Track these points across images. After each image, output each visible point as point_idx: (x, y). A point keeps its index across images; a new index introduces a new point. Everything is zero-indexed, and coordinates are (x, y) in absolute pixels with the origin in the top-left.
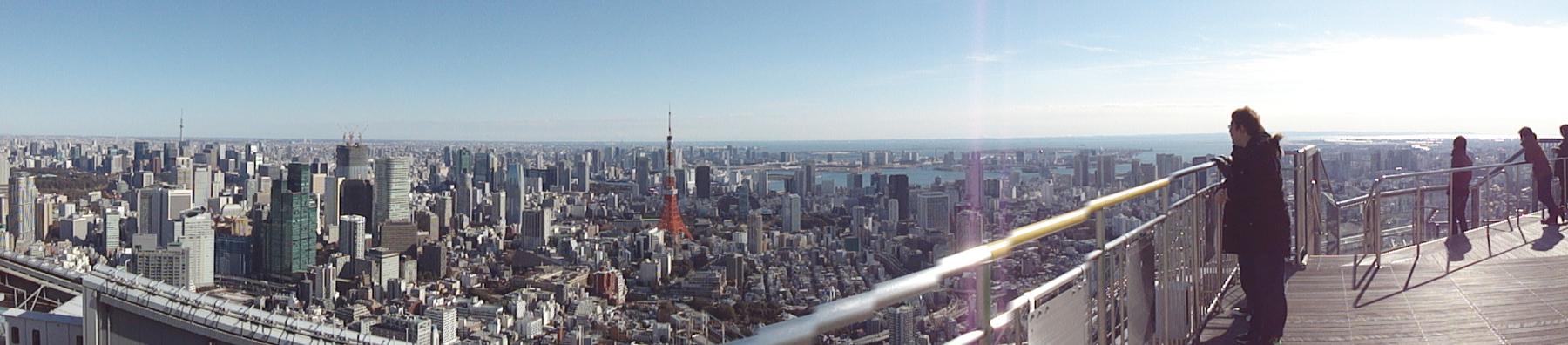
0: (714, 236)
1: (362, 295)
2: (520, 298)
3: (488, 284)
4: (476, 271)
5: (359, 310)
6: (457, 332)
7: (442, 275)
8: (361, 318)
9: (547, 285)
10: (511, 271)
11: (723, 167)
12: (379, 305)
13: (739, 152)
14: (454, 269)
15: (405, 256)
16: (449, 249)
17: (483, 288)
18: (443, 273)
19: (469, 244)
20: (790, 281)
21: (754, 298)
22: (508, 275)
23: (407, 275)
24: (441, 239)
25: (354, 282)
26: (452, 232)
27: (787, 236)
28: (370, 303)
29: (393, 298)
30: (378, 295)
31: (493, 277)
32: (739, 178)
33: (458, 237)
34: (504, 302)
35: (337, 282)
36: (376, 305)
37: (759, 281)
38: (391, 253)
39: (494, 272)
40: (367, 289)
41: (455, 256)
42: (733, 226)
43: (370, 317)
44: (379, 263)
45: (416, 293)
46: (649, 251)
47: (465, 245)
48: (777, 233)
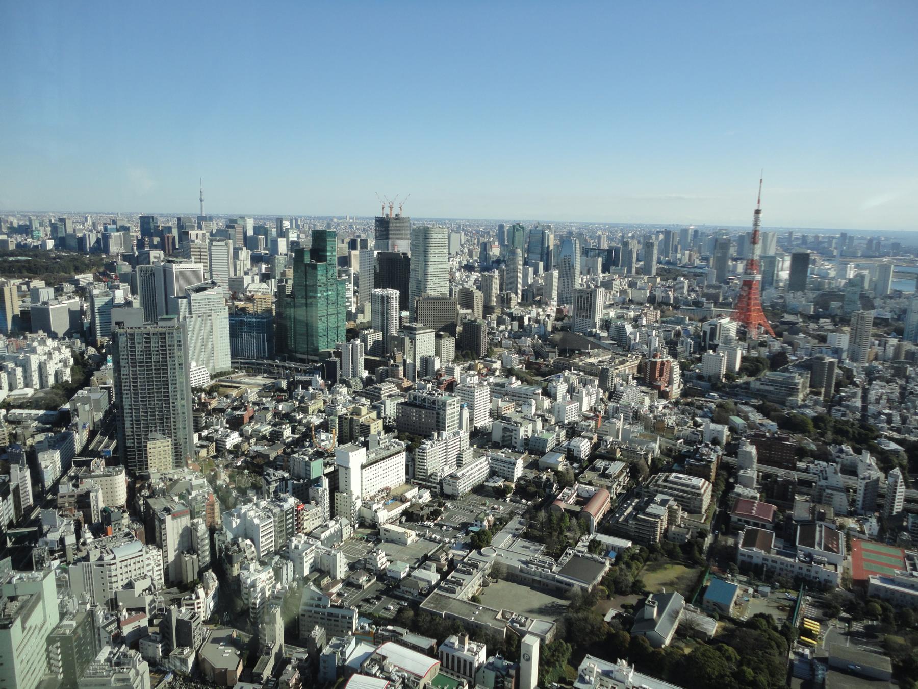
0: (801, 335)
1: (391, 373)
2: (561, 380)
3: (529, 365)
4: (520, 352)
6: (490, 413)
7: (482, 355)
8: (390, 396)
9: (591, 371)
11: (829, 256)
12: (411, 384)
13: (856, 242)
14: (496, 349)
15: (441, 333)
16: (493, 329)
18: (483, 352)
19: (516, 324)
20: (901, 403)
21: (844, 415)
23: (444, 352)
24: (484, 318)
25: (383, 360)
26: (498, 312)
27: (908, 346)
28: (400, 381)
29: (426, 376)
31: (537, 359)
32: (851, 272)
33: (504, 317)
34: (545, 384)
35: (365, 359)
36: (406, 383)
37: (854, 395)
38: (427, 328)
39: (538, 354)
40: (397, 366)
41: (498, 335)
42: (832, 327)
43: (398, 395)
44: (413, 340)
45: (450, 371)
46: (716, 342)
47: (511, 324)
48: (893, 341)
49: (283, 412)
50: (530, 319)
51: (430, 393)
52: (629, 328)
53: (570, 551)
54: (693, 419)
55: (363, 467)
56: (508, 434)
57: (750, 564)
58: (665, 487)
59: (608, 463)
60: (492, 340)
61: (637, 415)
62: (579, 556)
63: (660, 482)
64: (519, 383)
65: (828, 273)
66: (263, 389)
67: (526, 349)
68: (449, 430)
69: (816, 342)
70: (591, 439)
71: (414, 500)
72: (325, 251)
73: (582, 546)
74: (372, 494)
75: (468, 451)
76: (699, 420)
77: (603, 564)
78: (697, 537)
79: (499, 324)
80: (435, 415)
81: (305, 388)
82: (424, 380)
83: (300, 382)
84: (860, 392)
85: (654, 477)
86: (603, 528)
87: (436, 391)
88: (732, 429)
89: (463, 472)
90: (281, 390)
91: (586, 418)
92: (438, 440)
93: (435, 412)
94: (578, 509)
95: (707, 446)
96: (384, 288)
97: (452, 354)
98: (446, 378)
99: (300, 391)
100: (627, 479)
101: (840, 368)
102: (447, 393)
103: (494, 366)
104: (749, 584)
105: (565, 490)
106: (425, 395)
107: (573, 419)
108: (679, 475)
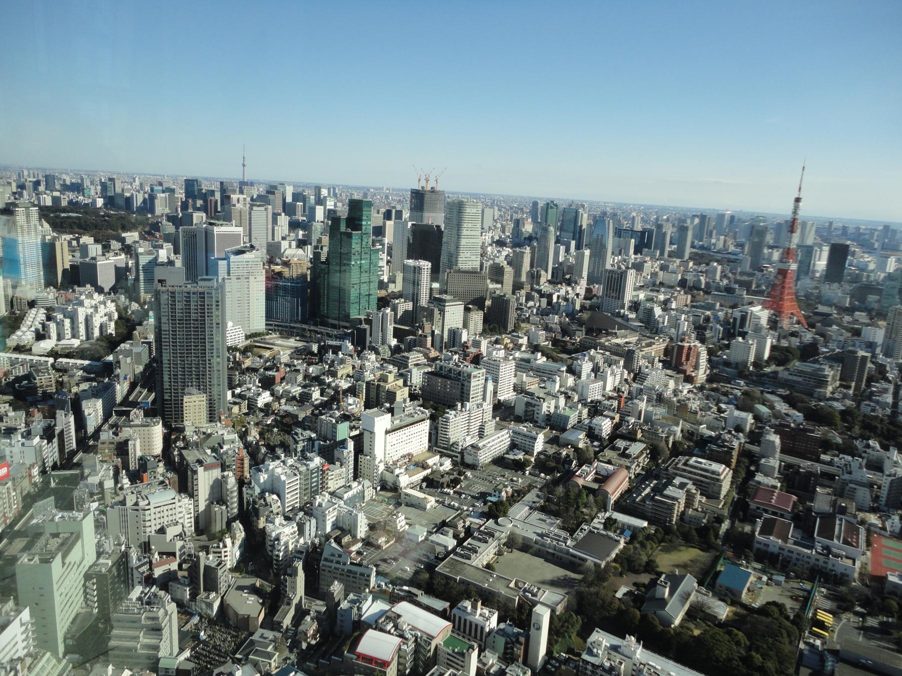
0: (835, 327)
1: (419, 343)
2: (587, 358)
3: (555, 342)
4: (547, 328)
5: (415, 357)
6: (514, 387)
7: (509, 329)
8: (417, 365)
9: (617, 351)
10: (584, 332)
12: (438, 354)
14: (523, 325)
15: (470, 306)
16: (521, 304)
17: (550, 346)
18: (510, 327)
19: (544, 301)
21: (873, 410)
22: (579, 337)
23: (472, 325)
24: (513, 293)
26: (527, 288)
28: (427, 351)
29: (453, 347)
30: (438, 344)
31: (563, 336)
33: (533, 293)
34: (570, 362)
35: (394, 327)
36: (433, 354)
37: (885, 391)
39: (565, 331)
40: (426, 336)
42: (867, 321)
43: (425, 365)
44: (442, 312)
45: (477, 344)
46: (745, 330)
47: (540, 301)
49: (313, 375)
50: (558, 297)
51: (456, 365)
52: (658, 311)
53: (586, 527)
54: (717, 405)
55: (387, 432)
56: (531, 408)
57: (766, 552)
58: (684, 470)
59: (628, 443)
60: (519, 316)
61: (660, 397)
62: (594, 532)
63: (680, 466)
64: (545, 359)
65: (867, 266)
66: (295, 352)
67: (553, 326)
68: (473, 402)
69: (849, 334)
70: (612, 418)
71: (435, 467)
72: (361, 220)
73: (598, 523)
74: (395, 459)
75: (490, 423)
76: (723, 406)
77: (618, 542)
78: (714, 522)
79: (527, 300)
80: (460, 386)
81: (335, 352)
82: (451, 352)
83: (331, 347)
84: (891, 388)
85: (674, 460)
86: (620, 507)
87: (462, 363)
88: (757, 418)
89: (484, 443)
90: (312, 354)
91: (610, 398)
92: (461, 411)
93: (460, 383)
94: (595, 486)
95: (730, 432)
96: (417, 259)
97: (480, 328)
98: (473, 350)
99: (330, 356)
100: (647, 460)
101: (873, 363)
102: (473, 365)
103: (521, 341)
104: (764, 571)
105: (584, 467)
106: (451, 365)
107: (596, 398)
108: (700, 460)
